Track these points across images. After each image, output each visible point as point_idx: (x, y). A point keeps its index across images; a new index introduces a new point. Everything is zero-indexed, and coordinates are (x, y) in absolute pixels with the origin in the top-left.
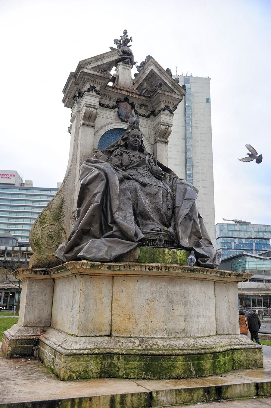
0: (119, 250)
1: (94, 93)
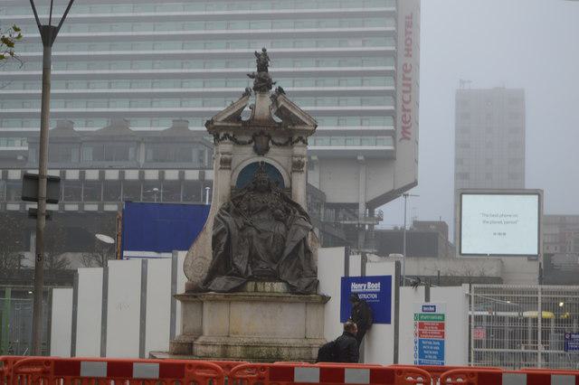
0: (233, 284)
1: (228, 140)
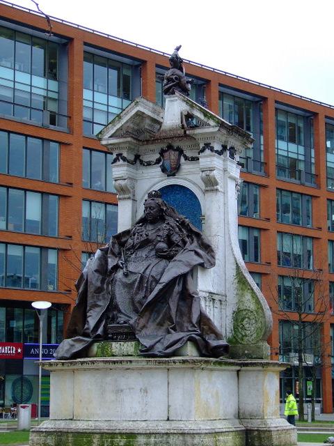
0: (79, 347)
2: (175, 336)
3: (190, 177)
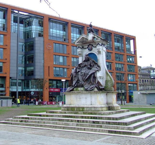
0: (71, 89)
1: (79, 48)
2: (92, 86)
3: (95, 51)
